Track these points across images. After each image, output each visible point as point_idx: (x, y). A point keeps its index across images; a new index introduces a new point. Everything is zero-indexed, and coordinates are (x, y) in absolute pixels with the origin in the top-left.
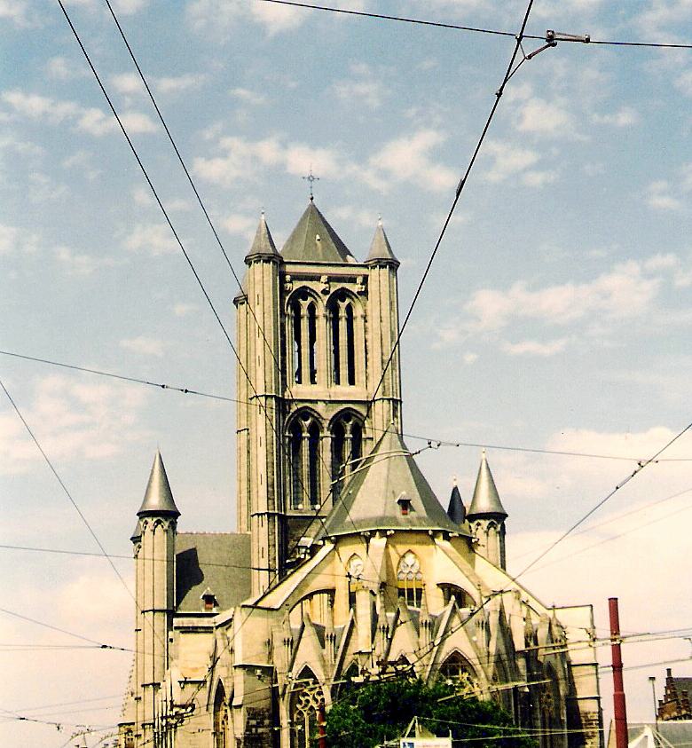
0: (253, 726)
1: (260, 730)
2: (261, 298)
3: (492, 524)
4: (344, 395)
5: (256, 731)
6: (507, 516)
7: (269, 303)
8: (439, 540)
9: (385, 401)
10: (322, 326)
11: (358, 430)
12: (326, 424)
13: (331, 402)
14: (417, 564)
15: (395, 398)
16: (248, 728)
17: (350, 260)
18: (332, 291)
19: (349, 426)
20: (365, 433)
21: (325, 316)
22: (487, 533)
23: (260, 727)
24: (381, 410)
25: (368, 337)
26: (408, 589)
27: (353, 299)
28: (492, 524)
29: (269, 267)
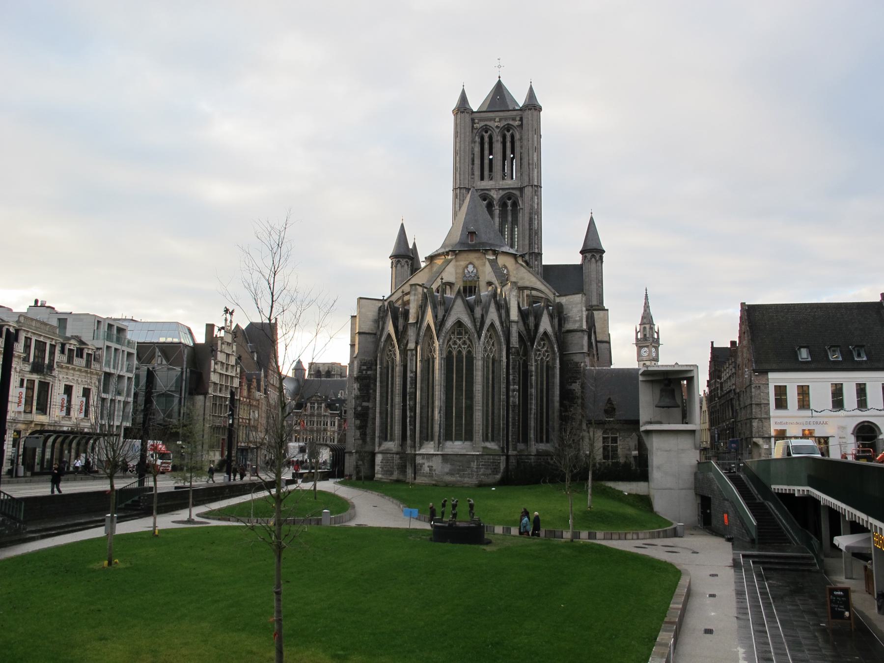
0: (364, 370)
1: (369, 372)
3: (593, 256)
4: (507, 185)
5: (366, 373)
6: (604, 252)
9: (530, 187)
11: (515, 204)
13: (499, 189)
15: (536, 184)
16: (360, 371)
18: (502, 125)
19: (509, 202)
22: (590, 261)
24: (528, 191)
28: (593, 256)
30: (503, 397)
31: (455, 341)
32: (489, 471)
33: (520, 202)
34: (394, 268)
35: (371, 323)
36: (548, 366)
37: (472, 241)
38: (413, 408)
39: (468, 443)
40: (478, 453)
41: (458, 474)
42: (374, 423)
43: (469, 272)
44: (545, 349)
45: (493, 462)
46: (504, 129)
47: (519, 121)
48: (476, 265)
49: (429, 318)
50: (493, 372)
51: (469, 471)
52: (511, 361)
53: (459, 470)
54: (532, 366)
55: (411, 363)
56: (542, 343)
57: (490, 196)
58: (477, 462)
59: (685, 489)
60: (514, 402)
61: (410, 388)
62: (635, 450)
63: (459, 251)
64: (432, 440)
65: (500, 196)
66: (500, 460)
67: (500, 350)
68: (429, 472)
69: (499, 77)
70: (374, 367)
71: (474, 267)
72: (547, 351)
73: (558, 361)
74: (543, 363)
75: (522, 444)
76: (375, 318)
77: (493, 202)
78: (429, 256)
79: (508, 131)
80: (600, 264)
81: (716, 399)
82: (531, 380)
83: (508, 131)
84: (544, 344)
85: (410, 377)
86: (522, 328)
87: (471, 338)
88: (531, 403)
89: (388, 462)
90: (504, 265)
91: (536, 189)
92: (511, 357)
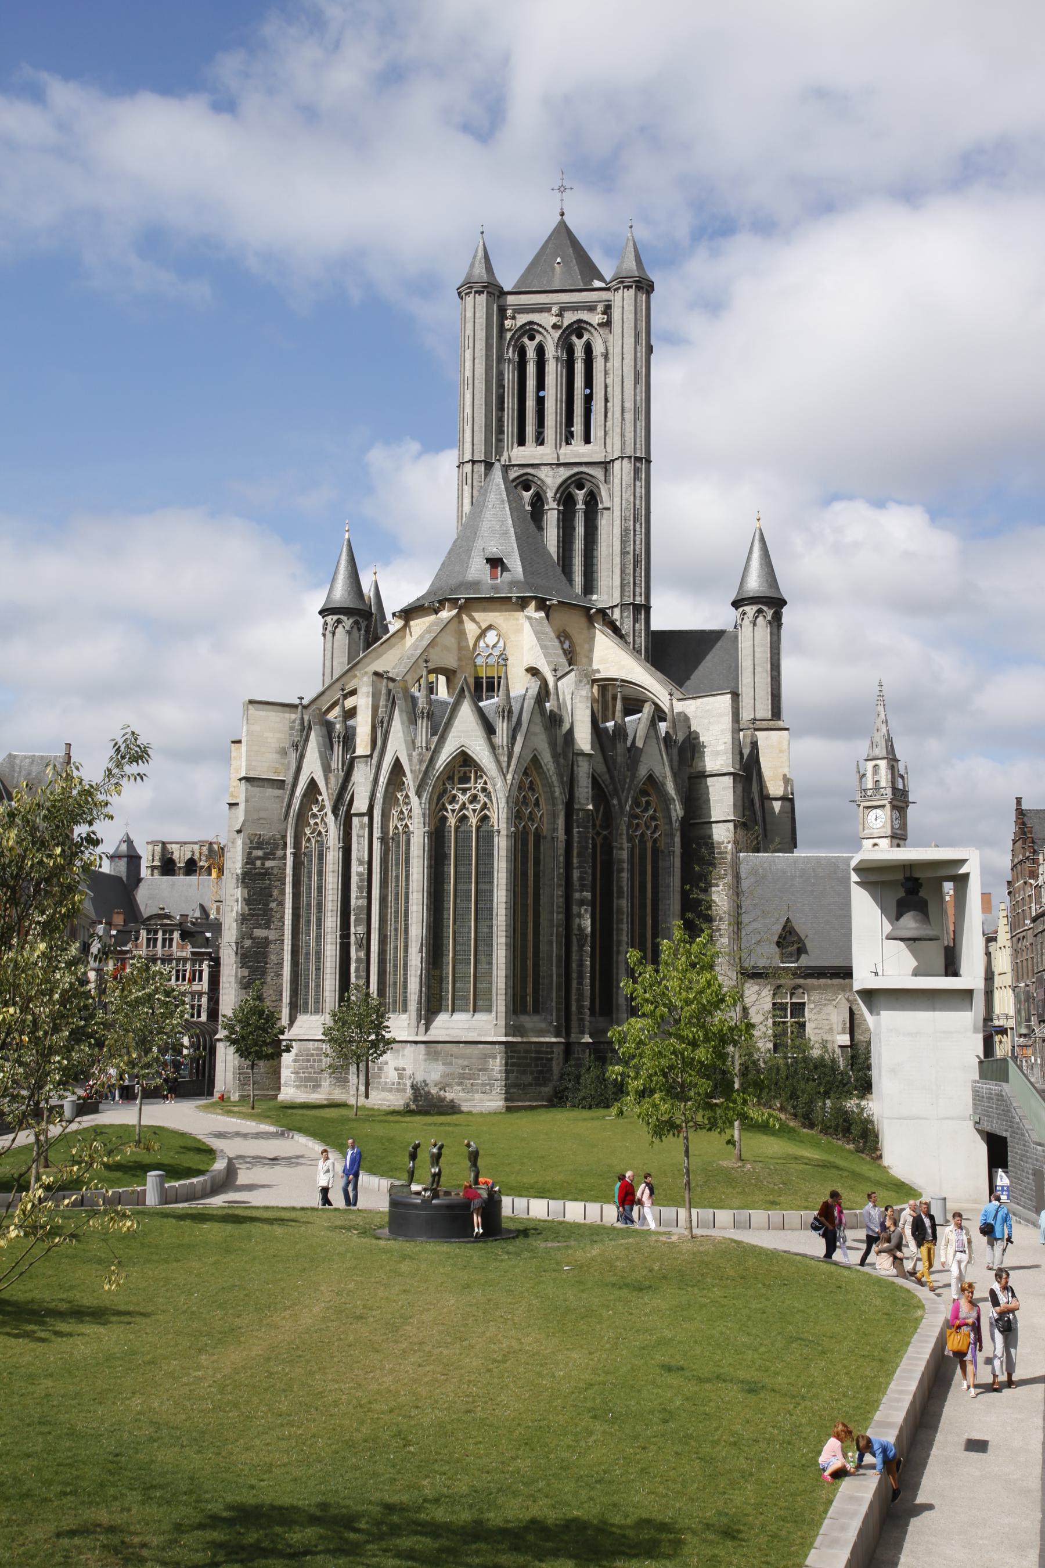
0: (259, 858)
1: (269, 864)
2: (471, 340)
3: (760, 611)
4: (576, 456)
5: (263, 864)
7: (481, 345)
8: (531, 610)
9: (626, 461)
10: (553, 371)
11: (592, 499)
12: (550, 494)
13: (559, 465)
14: (501, 644)
15: (638, 455)
16: (249, 860)
17: (597, 284)
18: (566, 324)
19: (580, 495)
20: (602, 502)
21: (557, 359)
23: (269, 859)
24: (622, 471)
25: (609, 381)
26: (487, 678)
27: (592, 334)
29: (482, 299)
30: (558, 917)
31: (455, 796)
32: (528, 1079)
33: (604, 493)
34: (329, 635)
35: (275, 756)
36: (655, 851)
37: (494, 577)
38: (364, 942)
39: (481, 1017)
40: (504, 1039)
41: (461, 1084)
42: (279, 975)
43: (488, 646)
44: (651, 812)
45: (537, 1059)
46: (571, 334)
47: (604, 313)
48: (503, 631)
49: (397, 745)
50: (537, 863)
51: (483, 1078)
52: (576, 839)
53: (462, 1077)
54: (621, 849)
55: (358, 843)
56: (644, 800)
57: (539, 479)
58: (501, 1059)
59: (952, 1119)
60: (581, 929)
61: (357, 898)
62: (844, 1033)
63: (466, 599)
64: (405, 1011)
65: (560, 480)
66: (552, 1052)
67: (554, 816)
68: (396, 1080)
69: (562, 214)
70: (279, 853)
71: (499, 635)
72: (653, 818)
73: (677, 839)
74: (645, 842)
75: (601, 1019)
76: (282, 745)
77: (546, 493)
78: (402, 611)
79: (580, 336)
80: (775, 630)
81: (1028, 922)
82: (619, 879)
83: (580, 336)
84: (648, 803)
85: (359, 874)
86: (601, 768)
87: (489, 787)
88: (620, 930)
89: (308, 1061)
90: (564, 631)
91: (638, 465)
92: (575, 830)
